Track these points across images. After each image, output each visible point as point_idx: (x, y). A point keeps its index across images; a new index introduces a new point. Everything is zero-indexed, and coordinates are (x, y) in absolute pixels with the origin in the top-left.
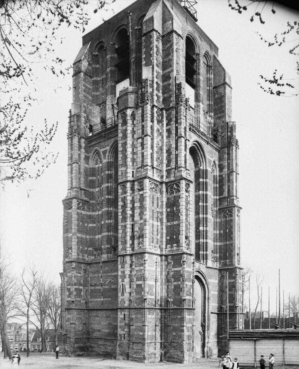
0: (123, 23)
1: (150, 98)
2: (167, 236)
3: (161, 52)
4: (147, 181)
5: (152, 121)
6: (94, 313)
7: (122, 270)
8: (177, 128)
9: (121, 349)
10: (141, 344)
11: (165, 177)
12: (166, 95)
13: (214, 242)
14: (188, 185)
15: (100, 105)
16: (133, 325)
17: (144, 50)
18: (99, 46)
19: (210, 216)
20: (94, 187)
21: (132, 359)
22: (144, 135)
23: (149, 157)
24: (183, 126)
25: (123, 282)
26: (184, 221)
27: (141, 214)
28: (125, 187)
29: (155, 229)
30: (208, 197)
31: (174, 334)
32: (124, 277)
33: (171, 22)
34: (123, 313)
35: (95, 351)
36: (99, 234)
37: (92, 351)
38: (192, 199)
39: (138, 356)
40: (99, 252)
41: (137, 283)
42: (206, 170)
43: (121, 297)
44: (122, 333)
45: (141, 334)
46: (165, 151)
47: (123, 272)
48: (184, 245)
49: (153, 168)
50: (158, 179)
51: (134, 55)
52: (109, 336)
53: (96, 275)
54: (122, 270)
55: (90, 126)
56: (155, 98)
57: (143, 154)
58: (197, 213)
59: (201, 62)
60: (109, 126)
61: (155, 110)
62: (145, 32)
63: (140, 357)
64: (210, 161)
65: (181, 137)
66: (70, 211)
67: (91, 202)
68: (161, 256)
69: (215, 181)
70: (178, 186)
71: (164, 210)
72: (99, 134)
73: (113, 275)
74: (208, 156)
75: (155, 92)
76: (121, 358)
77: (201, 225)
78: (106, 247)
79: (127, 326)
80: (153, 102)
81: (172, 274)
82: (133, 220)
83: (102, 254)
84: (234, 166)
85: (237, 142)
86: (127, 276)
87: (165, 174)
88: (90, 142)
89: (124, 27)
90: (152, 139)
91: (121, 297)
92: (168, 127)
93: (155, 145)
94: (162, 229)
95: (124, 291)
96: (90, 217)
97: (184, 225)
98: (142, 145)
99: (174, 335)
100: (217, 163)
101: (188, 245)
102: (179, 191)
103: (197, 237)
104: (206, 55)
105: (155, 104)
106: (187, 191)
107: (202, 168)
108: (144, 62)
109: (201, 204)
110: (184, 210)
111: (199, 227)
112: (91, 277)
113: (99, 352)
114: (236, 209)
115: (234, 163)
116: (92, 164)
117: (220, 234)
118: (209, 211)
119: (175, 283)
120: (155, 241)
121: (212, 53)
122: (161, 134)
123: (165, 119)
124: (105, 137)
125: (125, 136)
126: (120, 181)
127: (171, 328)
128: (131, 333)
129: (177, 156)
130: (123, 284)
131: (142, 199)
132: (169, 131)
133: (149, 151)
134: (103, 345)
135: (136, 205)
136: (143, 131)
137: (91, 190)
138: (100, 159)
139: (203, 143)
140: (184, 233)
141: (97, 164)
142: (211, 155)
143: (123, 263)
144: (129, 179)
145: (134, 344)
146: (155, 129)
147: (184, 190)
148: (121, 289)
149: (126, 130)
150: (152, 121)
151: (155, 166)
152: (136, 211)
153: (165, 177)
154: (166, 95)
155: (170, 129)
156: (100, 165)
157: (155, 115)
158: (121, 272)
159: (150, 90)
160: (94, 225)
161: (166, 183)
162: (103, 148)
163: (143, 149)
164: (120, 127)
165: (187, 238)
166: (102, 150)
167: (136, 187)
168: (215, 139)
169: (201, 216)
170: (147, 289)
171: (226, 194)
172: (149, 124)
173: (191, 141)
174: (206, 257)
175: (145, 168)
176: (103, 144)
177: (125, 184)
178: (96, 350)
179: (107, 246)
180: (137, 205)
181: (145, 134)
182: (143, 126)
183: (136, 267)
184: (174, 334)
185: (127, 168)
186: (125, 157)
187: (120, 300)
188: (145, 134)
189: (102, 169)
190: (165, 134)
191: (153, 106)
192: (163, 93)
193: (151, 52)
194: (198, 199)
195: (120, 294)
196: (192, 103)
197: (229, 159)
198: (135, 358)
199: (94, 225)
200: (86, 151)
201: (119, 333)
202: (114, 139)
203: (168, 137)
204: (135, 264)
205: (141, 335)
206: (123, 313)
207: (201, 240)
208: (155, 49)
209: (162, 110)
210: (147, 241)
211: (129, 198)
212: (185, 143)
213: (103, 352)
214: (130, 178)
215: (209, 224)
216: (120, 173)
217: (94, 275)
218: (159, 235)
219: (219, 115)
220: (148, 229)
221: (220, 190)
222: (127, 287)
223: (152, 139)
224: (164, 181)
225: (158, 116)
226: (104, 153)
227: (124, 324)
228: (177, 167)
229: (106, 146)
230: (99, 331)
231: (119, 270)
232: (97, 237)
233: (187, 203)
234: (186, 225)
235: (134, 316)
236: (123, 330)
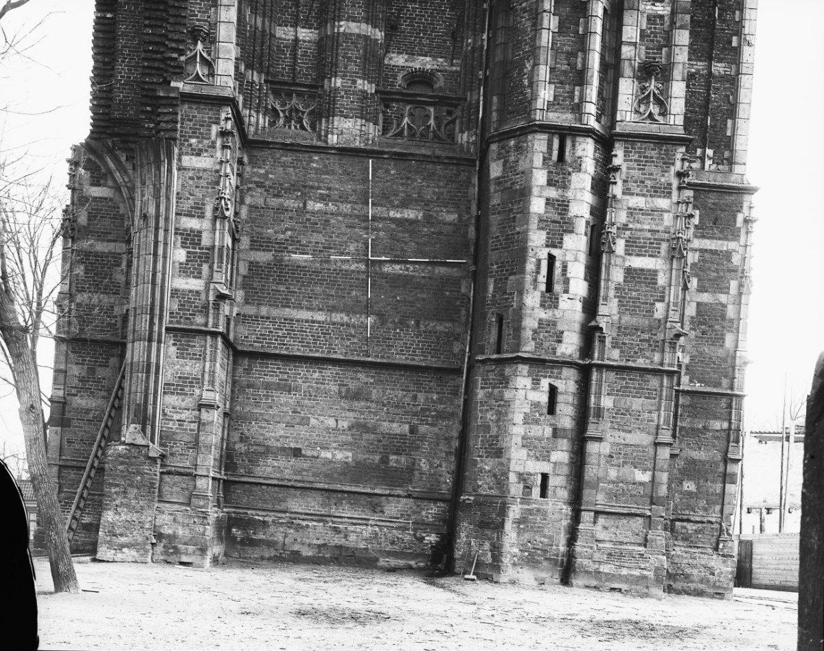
6: (270, 374)
7: (553, 193)
9: (527, 536)
10: (640, 520)
16: (600, 439)
21: (594, 583)
25: (554, 246)
32: (559, 226)
34: (545, 383)
35: (270, 544)
37: (253, 543)
39: (624, 572)
41: (627, 264)
43: (543, 315)
44: (536, 467)
47: (561, 206)
52: (356, 481)
53: (291, 203)
54: (553, 193)
63: (637, 573)
73: (393, 220)
76: (527, 576)
78: (360, 87)
86: (581, 226)
91: (543, 315)
95: (558, 288)
112: (253, 208)
113: (296, 548)
130: (551, 259)
134: (321, 518)
143: (560, 169)
148: (542, 278)
158: (549, 202)
178: (279, 538)
183: (628, 192)
187: (530, 323)
195: (532, 299)
198: (611, 577)
201: (515, 467)
204: (625, 181)
205: (641, 484)
206: (545, 383)
213: (319, 546)
217: (274, 202)
227: (548, 431)
230: (297, 453)
231: (535, 191)
232: (284, 33)
236: (546, 458)
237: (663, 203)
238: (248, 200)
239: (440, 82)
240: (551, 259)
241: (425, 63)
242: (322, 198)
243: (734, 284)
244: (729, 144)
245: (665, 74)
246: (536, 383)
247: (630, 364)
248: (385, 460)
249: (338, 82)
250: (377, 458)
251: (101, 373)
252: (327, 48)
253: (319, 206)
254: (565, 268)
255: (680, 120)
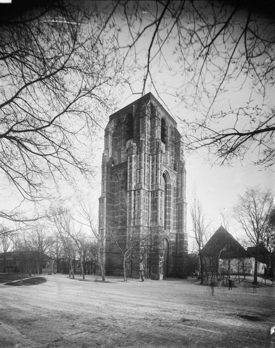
1: (144, 149)
2: (151, 217)
3: (150, 126)
4: (142, 191)
5: (145, 161)
8: (157, 165)
11: (150, 189)
12: (151, 148)
13: (173, 220)
14: (161, 193)
15: (117, 151)
17: (141, 125)
19: (171, 208)
20: (114, 192)
22: (140, 168)
23: (143, 179)
24: (160, 163)
26: (160, 211)
27: (139, 207)
28: (130, 194)
29: (145, 214)
30: (171, 198)
31: (154, 266)
36: (117, 215)
38: (163, 199)
40: (116, 224)
42: (170, 185)
45: (138, 265)
46: (151, 176)
48: (160, 222)
49: (145, 184)
50: (147, 190)
51: (136, 127)
55: (113, 161)
56: (146, 149)
57: (140, 177)
58: (165, 206)
59: (169, 130)
60: (122, 162)
61: (146, 155)
62: (141, 116)
64: (172, 180)
65: (159, 169)
67: (113, 199)
68: (148, 227)
69: (174, 190)
70: (157, 193)
71: (150, 205)
72: (117, 166)
74: (171, 178)
75: (146, 146)
77: (167, 212)
80: (145, 151)
82: (134, 210)
83: (118, 225)
84: (184, 183)
85: (185, 172)
87: (150, 187)
88: (113, 169)
89: (131, 112)
90: (145, 170)
92: (153, 164)
93: (146, 173)
94: (149, 214)
96: (112, 207)
97: (160, 212)
98: (140, 173)
100: (176, 181)
101: (161, 222)
102: (157, 196)
103: (165, 218)
104: (171, 127)
105: (146, 152)
106: (161, 196)
107: (168, 183)
108: (141, 131)
109: (167, 201)
110: (160, 205)
111: (166, 213)
114: (185, 204)
115: (184, 181)
116: (113, 181)
117: (176, 216)
118: (171, 205)
120: (145, 220)
121: (173, 126)
122: (149, 167)
123: (151, 160)
124: (120, 167)
125: (131, 168)
126: (128, 190)
129: (156, 178)
131: (139, 200)
132: (153, 166)
133: (143, 176)
136: (140, 165)
138: (118, 178)
139: (169, 171)
140: (159, 216)
141: (116, 180)
142: (173, 179)
144: (133, 189)
146: (146, 165)
147: (160, 195)
149: (132, 165)
150: (145, 161)
151: (146, 183)
153: (150, 189)
154: (151, 148)
155: (153, 165)
156: (118, 181)
157: (146, 158)
159: (144, 146)
160: (114, 211)
161: (151, 192)
163: (140, 174)
164: (129, 163)
165: (161, 219)
167: (137, 193)
168: (175, 169)
169: (167, 207)
170: (141, 244)
171: (180, 197)
172: (143, 162)
173: (164, 170)
174: (169, 228)
175: (141, 184)
179: (121, 222)
180: (137, 202)
181: (141, 167)
182: (140, 164)
184: (154, 266)
185: (132, 184)
186: (131, 178)
188: (141, 167)
189: (119, 183)
190: (151, 167)
191: (145, 154)
192: (151, 147)
193: (145, 127)
194: (166, 199)
196: (164, 151)
197: (181, 179)
200: (111, 174)
203: (152, 169)
207: (167, 220)
208: (147, 125)
209: (149, 155)
210: (141, 220)
211: (133, 199)
212: (161, 172)
214: (133, 188)
215: (171, 211)
216: (128, 186)
218: (147, 217)
219: (177, 157)
220: (142, 214)
221: (177, 195)
223: (145, 170)
224: (150, 190)
225: (148, 158)
226: (120, 175)
228: (157, 184)
229: (121, 172)
232: (116, 217)
233: (161, 202)
234: (161, 213)
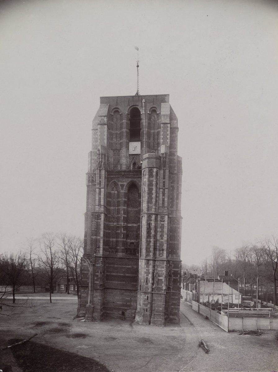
0: (137, 104)
18: (115, 110)
20: (110, 206)
33: (176, 121)
53: (112, 266)
54: (147, 268)
66: (99, 221)
73: (127, 268)
79: (149, 304)
81: (172, 272)
86: (151, 273)
99: (173, 308)
112: (107, 266)
119: (174, 278)
124: (123, 176)
127: (171, 303)
128: (153, 309)
130: (147, 278)
131: (162, 227)
135: (158, 230)
137: (109, 207)
141: (113, 190)
145: (155, 315)
152: (158, 233)
160: (110, 231)
162: (121, 182)
166: (120, 183)
167: (159, 219)
176: (121, 179)
177: (151, 215)
179: (122, 248)
184: (173, 307)
199: (110, 231)
202: (131, 179)
205: (161, 310)
206: (147, 296)
222: (151, 279)
227: (147, 303)
229: (123, 182)
232: (111, 239)
235: (156, 298)
236: (147, 306)
237: (163, 269)
238: (106, 265)
239: (135, 244)
240: (147, 278)
241: (133, 241)
242: (117, 265)
243: (179, 276)
244: (178, 253)
245: (163, 250)
246: (145, 295)
247: (159, 293)
248: (127, 303)
249: (119, 248)
250: (125, 303)
251: (86, 291)
252: (117, 241)
253: (116, 266)
254: (149, 279)
255: (165, 257)
